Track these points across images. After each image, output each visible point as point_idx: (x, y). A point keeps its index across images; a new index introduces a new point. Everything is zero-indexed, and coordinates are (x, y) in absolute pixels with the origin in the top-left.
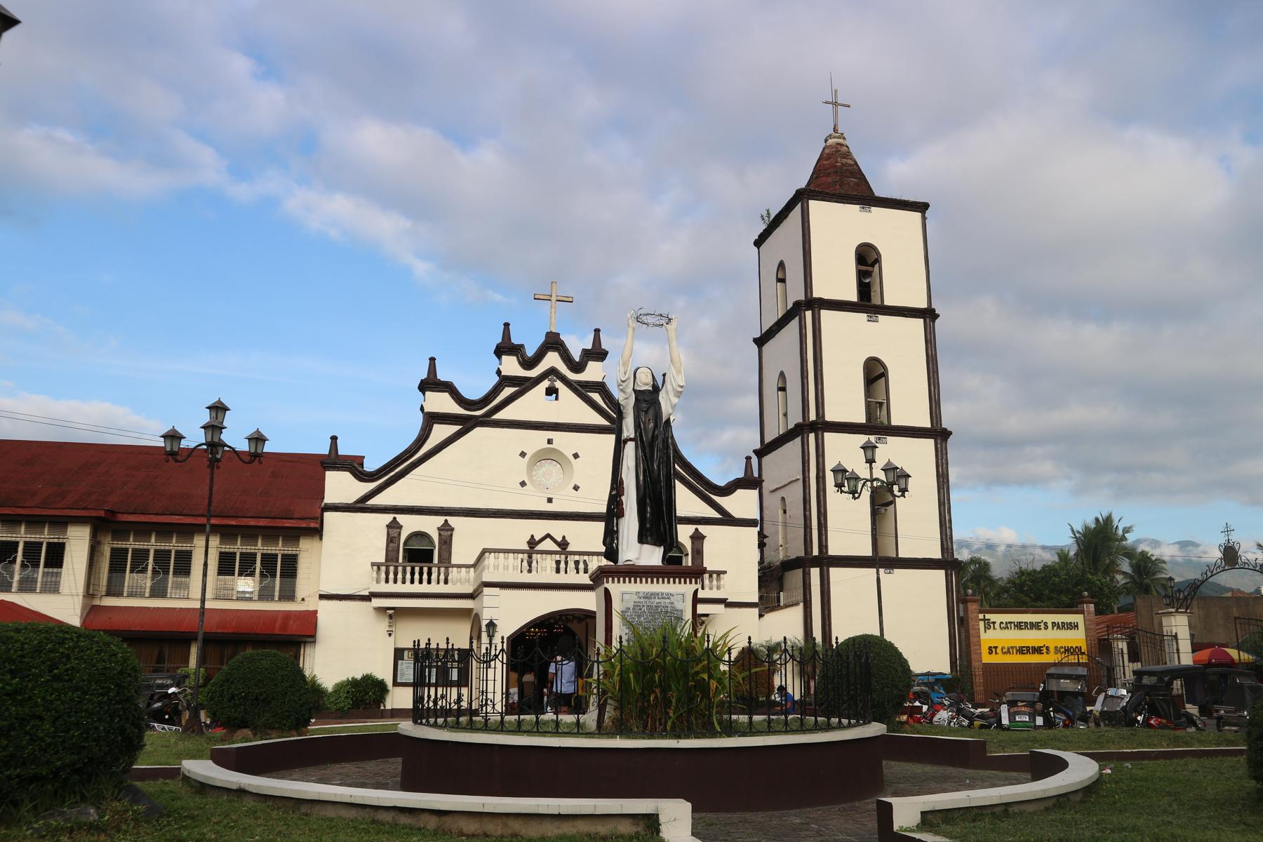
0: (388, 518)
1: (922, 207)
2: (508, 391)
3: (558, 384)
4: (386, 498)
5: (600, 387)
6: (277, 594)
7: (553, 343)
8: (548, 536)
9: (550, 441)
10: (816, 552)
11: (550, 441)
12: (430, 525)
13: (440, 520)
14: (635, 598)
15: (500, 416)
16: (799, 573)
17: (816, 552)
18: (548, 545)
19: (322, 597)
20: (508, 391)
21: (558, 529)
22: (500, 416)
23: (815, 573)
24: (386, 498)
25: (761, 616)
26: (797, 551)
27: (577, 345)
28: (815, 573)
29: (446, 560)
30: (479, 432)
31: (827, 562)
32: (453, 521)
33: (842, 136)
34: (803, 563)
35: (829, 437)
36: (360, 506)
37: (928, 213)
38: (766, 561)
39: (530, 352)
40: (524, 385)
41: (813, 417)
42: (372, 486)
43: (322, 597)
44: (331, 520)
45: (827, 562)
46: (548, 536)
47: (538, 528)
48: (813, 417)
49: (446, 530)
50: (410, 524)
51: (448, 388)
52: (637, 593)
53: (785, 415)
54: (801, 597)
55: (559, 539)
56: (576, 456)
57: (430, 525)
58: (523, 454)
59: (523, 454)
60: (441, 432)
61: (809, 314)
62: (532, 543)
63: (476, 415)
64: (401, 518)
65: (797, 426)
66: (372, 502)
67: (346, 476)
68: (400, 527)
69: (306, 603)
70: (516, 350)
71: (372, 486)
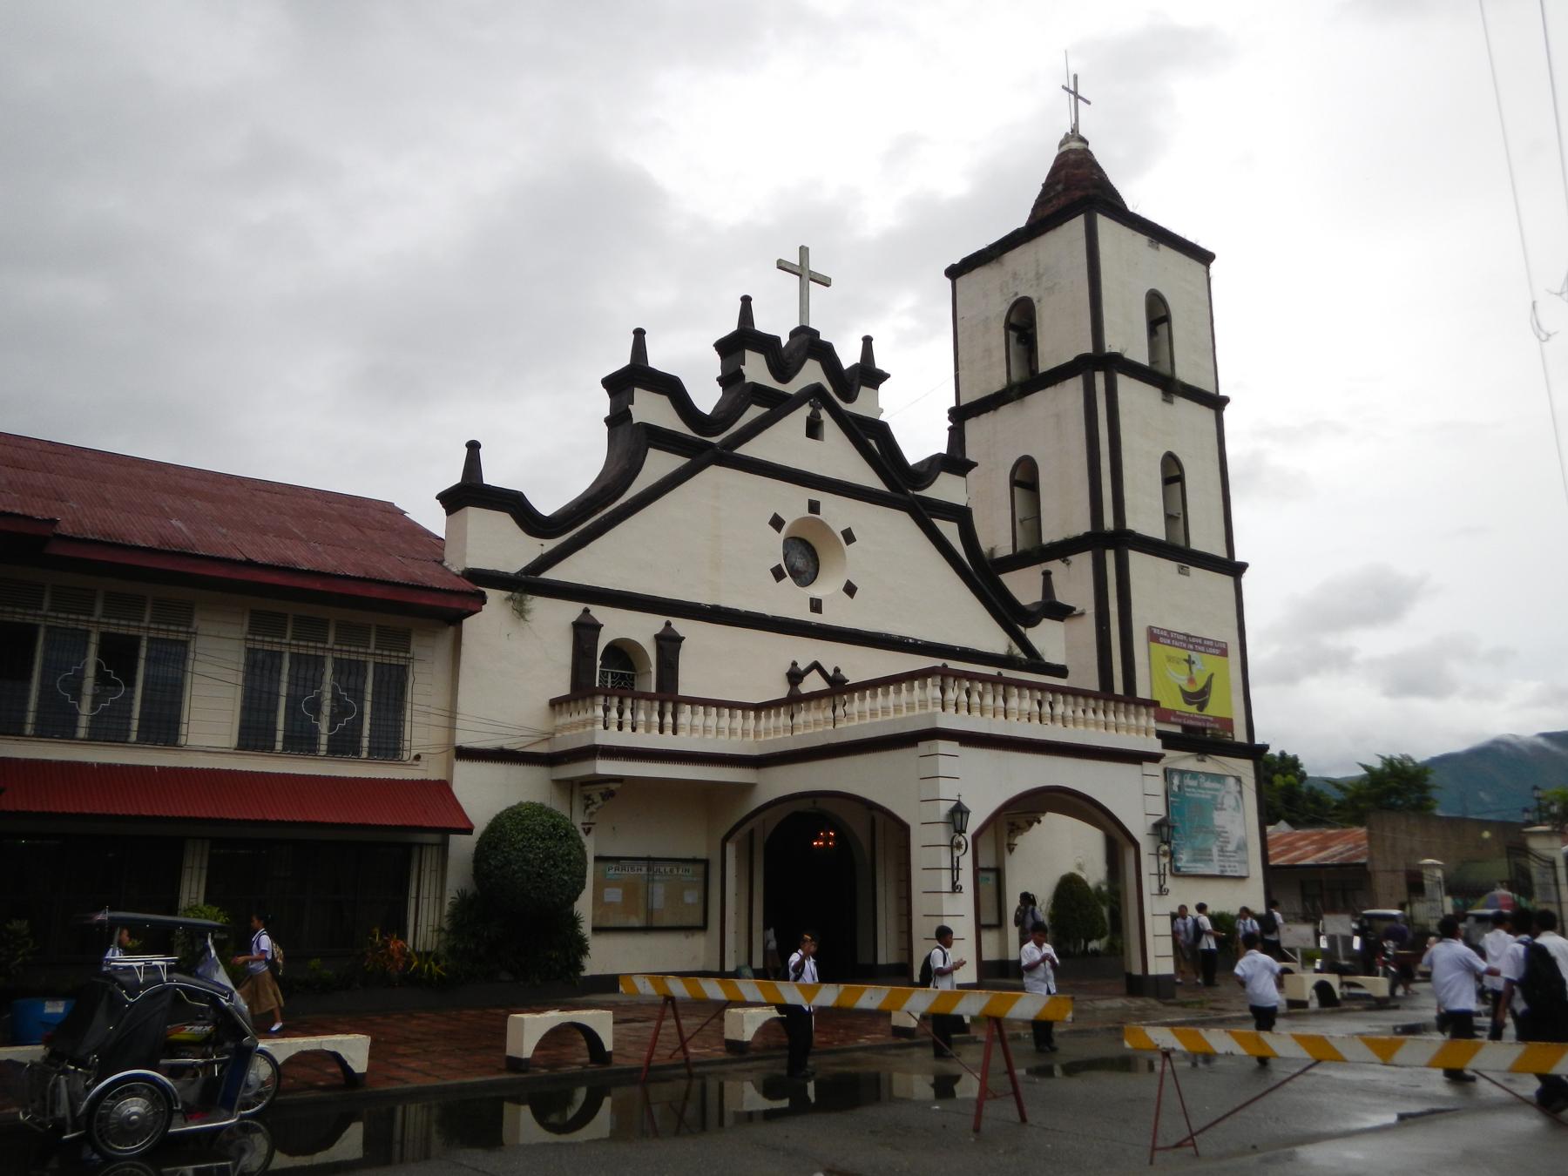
1: (1205, 258)
2: (754, 412)
3: (824, 415)
5: (881, 431)
6: (365, 743)
7: (810, 344)
8: (816, 666)
9: (814, 507)
11: (814, 507)
13: (656, 623)
18: (813, 683)
19: (465, 754)
20: (754, 412)
21: (834, 656)
27: (849, 356)
29: (668, 694)
30: (714, 475)
32: (680, 625)
33: (1083, 140)
35: (1136, 559)
36: (527, 585)
37: (1212, 265)
40: (778, 406)
41: (1109, 523)
42: (550, 545)
43: (465, 754)
46: (816, 666)
47: (805, 651)
48: (1109, 523)
49: (669, 644)
50: (616, 625)
51: (671, 387)
55: (831, 673)
56: (849, 537)
57: (641, 629)
58: (777, 523)
59: (777, 523)
60: (659, 464)
61: (1100, 378)
62: (795, 676)
63: (707, 443)
64: (599, 613)
66: (550, 575)
67: (503, 522)
68: (597, 627)
69: (422, 764)
70: (767, 344)
71: (550, 545)
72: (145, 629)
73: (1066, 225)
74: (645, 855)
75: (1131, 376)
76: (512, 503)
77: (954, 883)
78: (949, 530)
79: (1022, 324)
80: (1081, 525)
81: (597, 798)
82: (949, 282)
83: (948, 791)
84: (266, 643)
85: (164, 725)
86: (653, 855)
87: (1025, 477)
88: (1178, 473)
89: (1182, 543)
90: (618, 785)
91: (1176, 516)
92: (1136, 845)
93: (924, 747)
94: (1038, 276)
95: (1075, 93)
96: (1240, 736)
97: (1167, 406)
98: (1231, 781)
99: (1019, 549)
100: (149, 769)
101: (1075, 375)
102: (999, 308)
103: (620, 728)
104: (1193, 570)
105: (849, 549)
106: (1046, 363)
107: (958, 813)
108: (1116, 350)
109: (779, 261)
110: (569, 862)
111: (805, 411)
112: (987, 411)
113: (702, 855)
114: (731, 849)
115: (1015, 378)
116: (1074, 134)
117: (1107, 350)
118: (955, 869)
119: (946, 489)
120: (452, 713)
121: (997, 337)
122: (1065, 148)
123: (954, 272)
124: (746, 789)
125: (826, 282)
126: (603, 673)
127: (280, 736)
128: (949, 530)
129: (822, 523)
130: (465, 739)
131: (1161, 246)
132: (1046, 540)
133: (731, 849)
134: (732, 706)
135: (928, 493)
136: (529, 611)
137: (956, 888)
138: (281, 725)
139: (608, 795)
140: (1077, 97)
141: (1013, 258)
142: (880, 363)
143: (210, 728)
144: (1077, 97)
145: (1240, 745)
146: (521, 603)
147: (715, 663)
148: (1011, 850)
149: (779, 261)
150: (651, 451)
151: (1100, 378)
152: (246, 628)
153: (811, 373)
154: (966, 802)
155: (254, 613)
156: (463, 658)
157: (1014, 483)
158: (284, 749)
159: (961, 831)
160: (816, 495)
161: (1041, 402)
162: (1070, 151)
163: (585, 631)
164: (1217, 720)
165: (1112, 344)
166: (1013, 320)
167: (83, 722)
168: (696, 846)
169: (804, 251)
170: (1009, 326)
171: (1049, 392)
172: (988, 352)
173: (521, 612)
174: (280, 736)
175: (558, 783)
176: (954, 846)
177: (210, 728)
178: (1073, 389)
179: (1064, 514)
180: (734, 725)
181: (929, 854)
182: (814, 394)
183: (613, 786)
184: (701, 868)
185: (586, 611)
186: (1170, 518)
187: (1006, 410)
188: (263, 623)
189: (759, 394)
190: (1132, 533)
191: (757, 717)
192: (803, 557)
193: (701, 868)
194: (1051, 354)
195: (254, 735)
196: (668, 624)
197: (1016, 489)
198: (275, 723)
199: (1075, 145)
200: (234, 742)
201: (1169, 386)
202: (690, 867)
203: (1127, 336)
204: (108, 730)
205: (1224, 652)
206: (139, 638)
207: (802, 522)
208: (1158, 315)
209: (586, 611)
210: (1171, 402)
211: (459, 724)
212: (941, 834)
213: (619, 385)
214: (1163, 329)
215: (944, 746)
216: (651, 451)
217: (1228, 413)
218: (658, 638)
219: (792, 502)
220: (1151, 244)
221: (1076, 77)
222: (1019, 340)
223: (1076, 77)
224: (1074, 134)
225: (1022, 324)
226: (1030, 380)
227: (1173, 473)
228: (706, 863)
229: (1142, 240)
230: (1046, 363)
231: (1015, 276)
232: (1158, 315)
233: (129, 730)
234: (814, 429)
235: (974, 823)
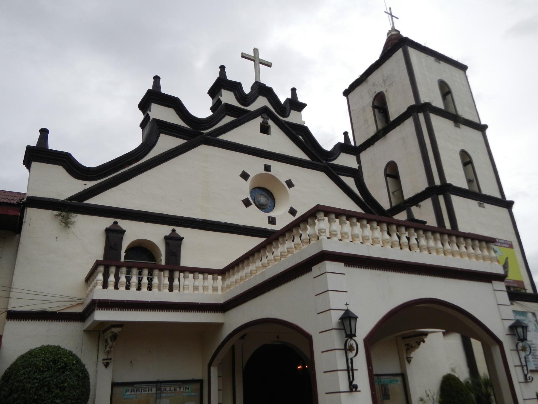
0: (108, 222)
2: (227, 119)
3: (270, 122)
4: (106, 199)
5: (304, 131)
7: (261, 89)
9: (267, 168)
11: (267, 168)
12: (156, 234)
13: (167, 230)
15: (226, 137)
19: (13, 315)
20: (227, 119)
22: (226, 137)
24: (106, 199)
27: (283, 96)
30: (203, 150)
32: (181, 231)
37: (468, 72)
39: (247, 90)
40: (242, 117)
41: (437, 182)
42: (90, 184)
43: (13, 315)
44: (36, 220)
48: (437, 182)
49: (174, 243)
50: (134, 232)
51: (174, 103)
56: (290, 184)
58: (245, 176)
59: (245, 176)
60: (166, 143)
61: (421, 116)
64: (123, 224)
67: (58, 172)
68: (122, 232)
70: (235, 87)
71: (90, 184)
73: (394, 55)
74: (155, 380)
75: (437, 115)
76: (65, 161)
77: (351, 383)
78: (350, 181)
79: (380, 104)
80: (422, 185)
81: (109, 340)
82: (345, 98)
83: (338, 303)
86: (161, 379)
87: (392, 172)
88: (469, 160)
89: (477, 191)
90: (119, 329)
91: (472, 179)
92: (500, 343)
93: (316, 269)
94: (384, 81)
95: (391, 14)
96: (530, 290)
97: (457, 129)
98: (530, 315)
99: (393, 205)
101: (409, 117)
102: (368, 100)
103: (116, 287)
104: (486, 205)
105: (290, 191)
106: (394, 115)
107: (348, 319)
108: (426, 101)
109: (242, 53)
110: (63, 389)
111: (259, 120)
112: (369, 146)
113: (198, 377)
114: (214, 371)
115: (380, 127)
116: (393, 29)
117: (422, 102)
118: (350, 370)
119: (346, 160)
120: (9, 288)
121: (370, 113)
122: (390, 35)
123: (346, 93)
124: (219, 326)
125: (269, 65)
126: (121, 257)
128: (350, 181)
129: (273, 177)
130: (16, 305)
131: (441, 62)
132: (406, 197)
133: (214, 371)
134: (203, 271)
135: (336, 162)
136: (73, 223)
137: (353, 388)
139: (114, 337)
140: (392, 16)
141: (372, 78)
142: (301, 99)
144: (392, 16)
145: (530, 295)
146: (68, 218)
147: (198, 248)
148: (409, 362)
149: (242, 53)
150: (162, 136)
151: (421, 116)
153: (261, 102)
154: (354, 310)
156: (19, 252)
157: (387, 175)
159: (351, 335)
160: (268, 162)
161: (394, 135)
162: (392, 35)
163: (114, 236)
164: (515, 281)
165: (424, 99)
166: (376, 104)
168: (193, 370)
169: (256, 51)
170: (374, 107)
171: (398, 129)
172: (366, 121)
173: (67, 224)
175: (88, 332)
176: (347, 349)
178: (409, 125)
179: (413, 182)
180: (206, 284)
181: (327, 360)
182: (264, 111)
183: (116, 330)
184: (197, 386)
185: (116, 223)
186: (469, 181)
187: (378, 144)
189: (229, 109)
190: (450, 185)
191: (223, 279)
192: (264, 195)
193: (197, 386)
194: (394, 113)
196: (174, 231)
197: (388, 178)
199: (394, 33)
201: (457, 120)
202: (191, 387)
203: (431, 95)
205: (511, 246)
207: (260, 176)
208: (445, 91)
209: (116, 223)
210: (459, 127)
211: (12, 295)
212: (335, 340)
213: (144, 106)
214: (449, 97)
215: (329, 266)
216: (162, 136)
217: (488, 132)
218: (166, 238)
219: (255, 166)
220: (436, 61)
221: (390, 9)
222: (380, 112)
223: (390, 9)
224: (393, 29)
225: (380, 104)
226: (387, 125)
227: (467, 160)
228: (201, 382)
229: (431, 59)
230: (394, 115)
231: (374, 85)
232: (445, 91)
234: (265, 129)
235: (363, 328)
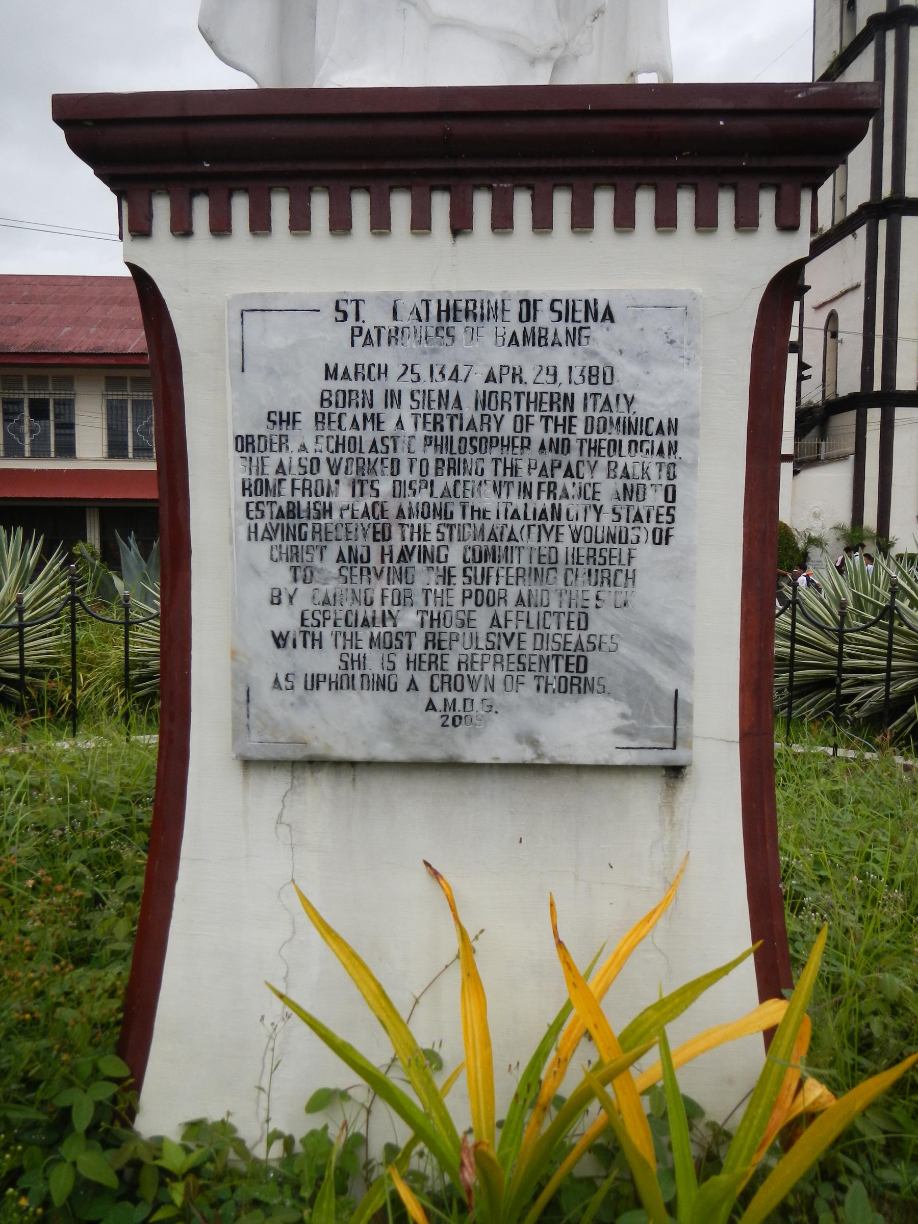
10: (877, 386)
14: (334, 343)
16: (850, 417)
17: (877, 386)
23: (874, 415)
25: (796, 473)
26: (849, 383)
28: (874, 415)
31: (891, 399)
34: (858, 403)
38: (804, 401)
45: (891, 399)
52: (345, 310)
53: (844, 198)
54: (851, 448)
65: (863, 207)
72: (51, 395)
84: (116, 396)
85: (67, 449)
99: (836, 223)
100: (60, 471)
127: (130, 449)
138: (130, 443)
143: (91, 447)
152: (103, 388)
155: (108, 379)
158: (134, 456)
167: (27, 448)
174: (130, 449)
177: (91, 447)
188: (114, 383)
195: (116, 449)
198: (127, 442)
200: (105, 455)
204: (39, 452)
206: (48, 400)
233: (50, 451)
